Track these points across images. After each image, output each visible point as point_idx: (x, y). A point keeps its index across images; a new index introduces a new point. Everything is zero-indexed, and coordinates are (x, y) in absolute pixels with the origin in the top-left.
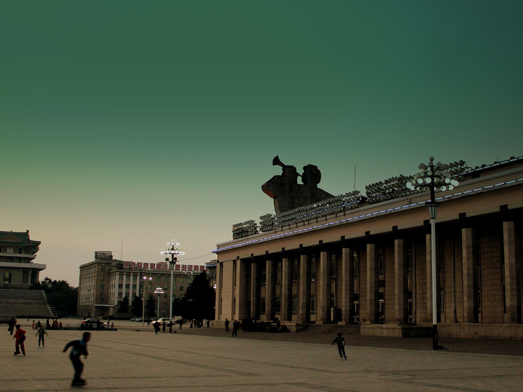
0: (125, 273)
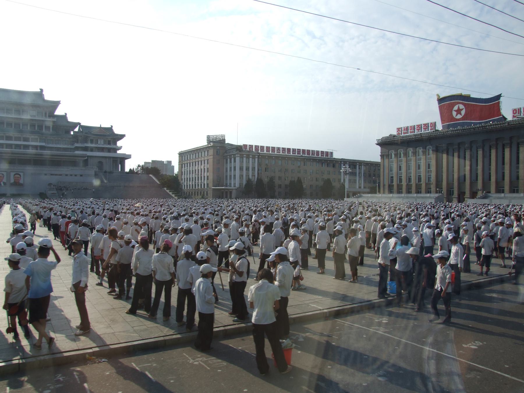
0: (245, 156)
